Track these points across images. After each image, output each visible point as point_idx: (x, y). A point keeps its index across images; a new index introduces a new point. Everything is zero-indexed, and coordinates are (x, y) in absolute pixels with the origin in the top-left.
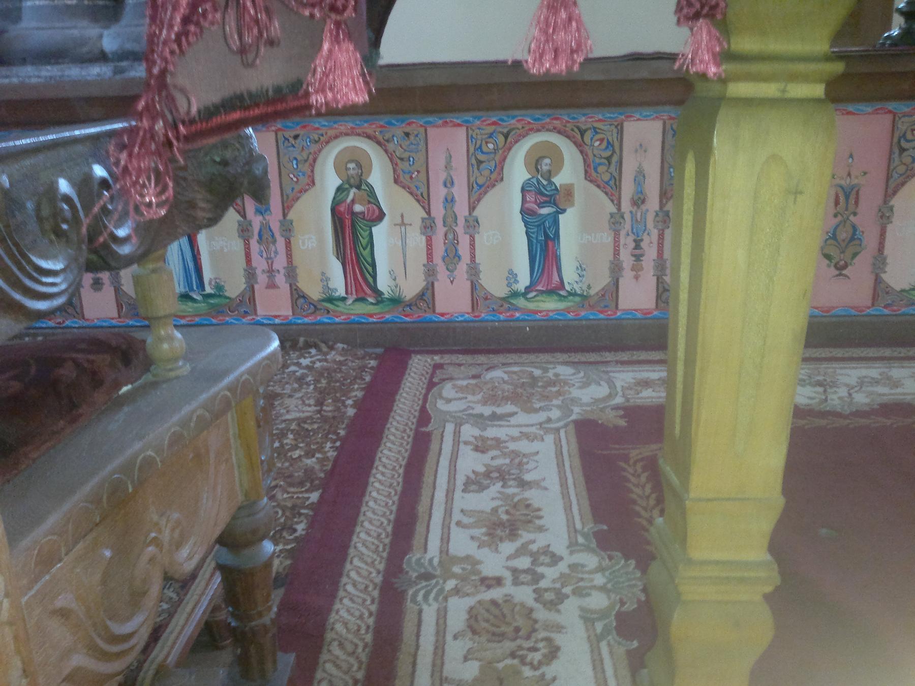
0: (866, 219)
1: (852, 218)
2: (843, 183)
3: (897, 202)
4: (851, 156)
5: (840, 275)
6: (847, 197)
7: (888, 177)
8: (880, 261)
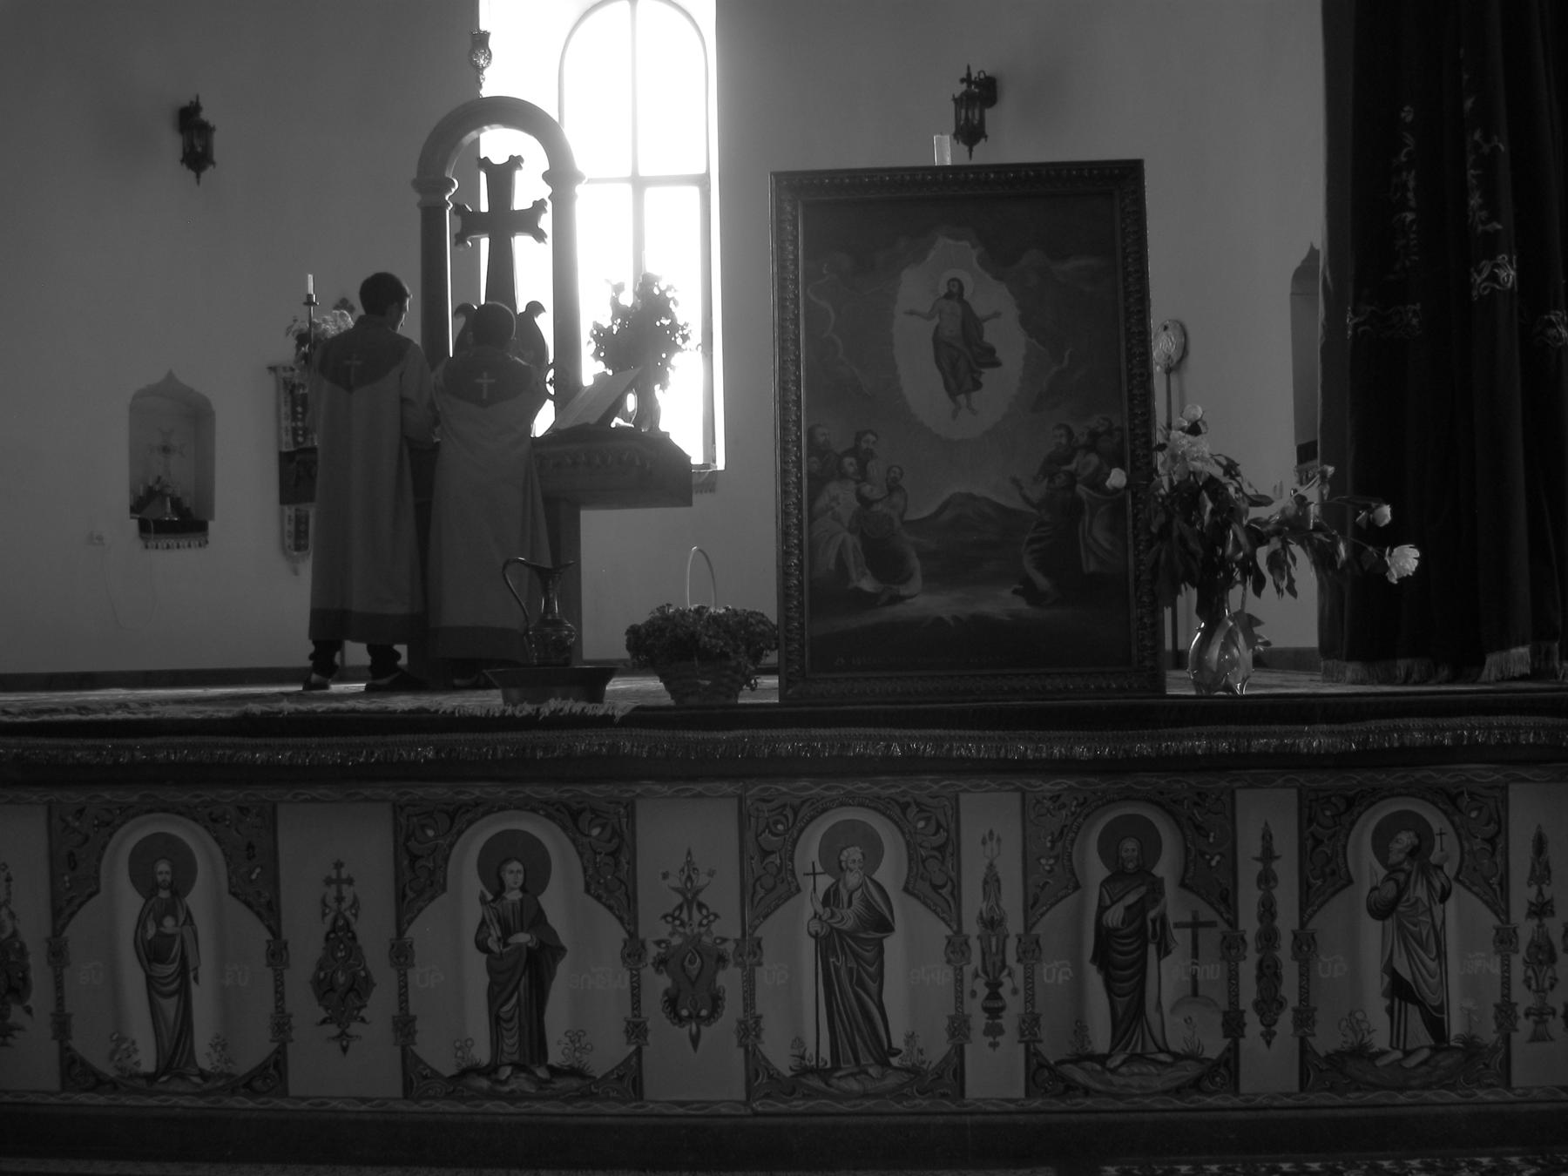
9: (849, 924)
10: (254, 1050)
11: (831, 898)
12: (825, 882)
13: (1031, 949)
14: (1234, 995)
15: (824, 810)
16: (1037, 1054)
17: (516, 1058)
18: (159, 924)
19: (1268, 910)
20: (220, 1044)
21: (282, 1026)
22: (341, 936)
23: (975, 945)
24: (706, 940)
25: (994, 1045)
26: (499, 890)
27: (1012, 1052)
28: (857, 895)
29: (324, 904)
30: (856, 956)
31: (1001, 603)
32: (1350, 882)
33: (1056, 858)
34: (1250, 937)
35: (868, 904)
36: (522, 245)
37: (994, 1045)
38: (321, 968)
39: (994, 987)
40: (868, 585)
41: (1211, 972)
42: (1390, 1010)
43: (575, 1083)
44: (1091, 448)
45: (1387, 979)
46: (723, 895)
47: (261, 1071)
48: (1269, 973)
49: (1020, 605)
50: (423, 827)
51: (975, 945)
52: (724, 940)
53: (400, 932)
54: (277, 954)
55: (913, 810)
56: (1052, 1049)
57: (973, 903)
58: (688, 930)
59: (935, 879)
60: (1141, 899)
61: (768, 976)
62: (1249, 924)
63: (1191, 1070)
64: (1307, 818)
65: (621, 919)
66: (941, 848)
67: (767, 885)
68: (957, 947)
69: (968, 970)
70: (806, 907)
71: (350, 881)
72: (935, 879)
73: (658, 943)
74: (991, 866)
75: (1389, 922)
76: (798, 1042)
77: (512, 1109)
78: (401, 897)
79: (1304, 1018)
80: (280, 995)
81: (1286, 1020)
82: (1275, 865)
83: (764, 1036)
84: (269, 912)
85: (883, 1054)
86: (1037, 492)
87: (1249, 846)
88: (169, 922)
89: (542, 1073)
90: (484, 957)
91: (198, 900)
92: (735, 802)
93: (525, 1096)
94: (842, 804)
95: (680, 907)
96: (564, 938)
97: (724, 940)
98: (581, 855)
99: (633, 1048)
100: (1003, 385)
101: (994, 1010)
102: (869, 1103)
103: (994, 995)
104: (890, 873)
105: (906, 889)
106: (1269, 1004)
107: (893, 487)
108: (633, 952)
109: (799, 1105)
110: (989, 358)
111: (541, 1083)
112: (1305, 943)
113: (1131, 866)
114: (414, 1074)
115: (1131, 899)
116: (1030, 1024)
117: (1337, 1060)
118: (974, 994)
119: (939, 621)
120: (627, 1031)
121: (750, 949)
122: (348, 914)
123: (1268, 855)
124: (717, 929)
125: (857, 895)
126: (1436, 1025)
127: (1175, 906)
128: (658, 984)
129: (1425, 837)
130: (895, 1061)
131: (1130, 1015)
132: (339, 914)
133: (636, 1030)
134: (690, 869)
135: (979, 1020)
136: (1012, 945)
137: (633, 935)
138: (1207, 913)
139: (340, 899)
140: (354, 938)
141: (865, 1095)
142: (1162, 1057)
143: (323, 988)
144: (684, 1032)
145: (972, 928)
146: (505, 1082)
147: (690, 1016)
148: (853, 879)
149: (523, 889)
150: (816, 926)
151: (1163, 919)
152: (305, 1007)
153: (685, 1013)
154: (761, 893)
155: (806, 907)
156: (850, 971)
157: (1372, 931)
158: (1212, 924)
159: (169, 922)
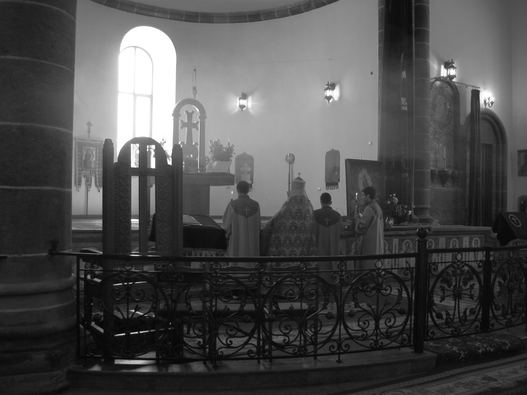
36: (194, 130)
64: (399, 242)
87: (394, 245)
123: (396, 247)
126: (409, 266)
129: (409, 244)
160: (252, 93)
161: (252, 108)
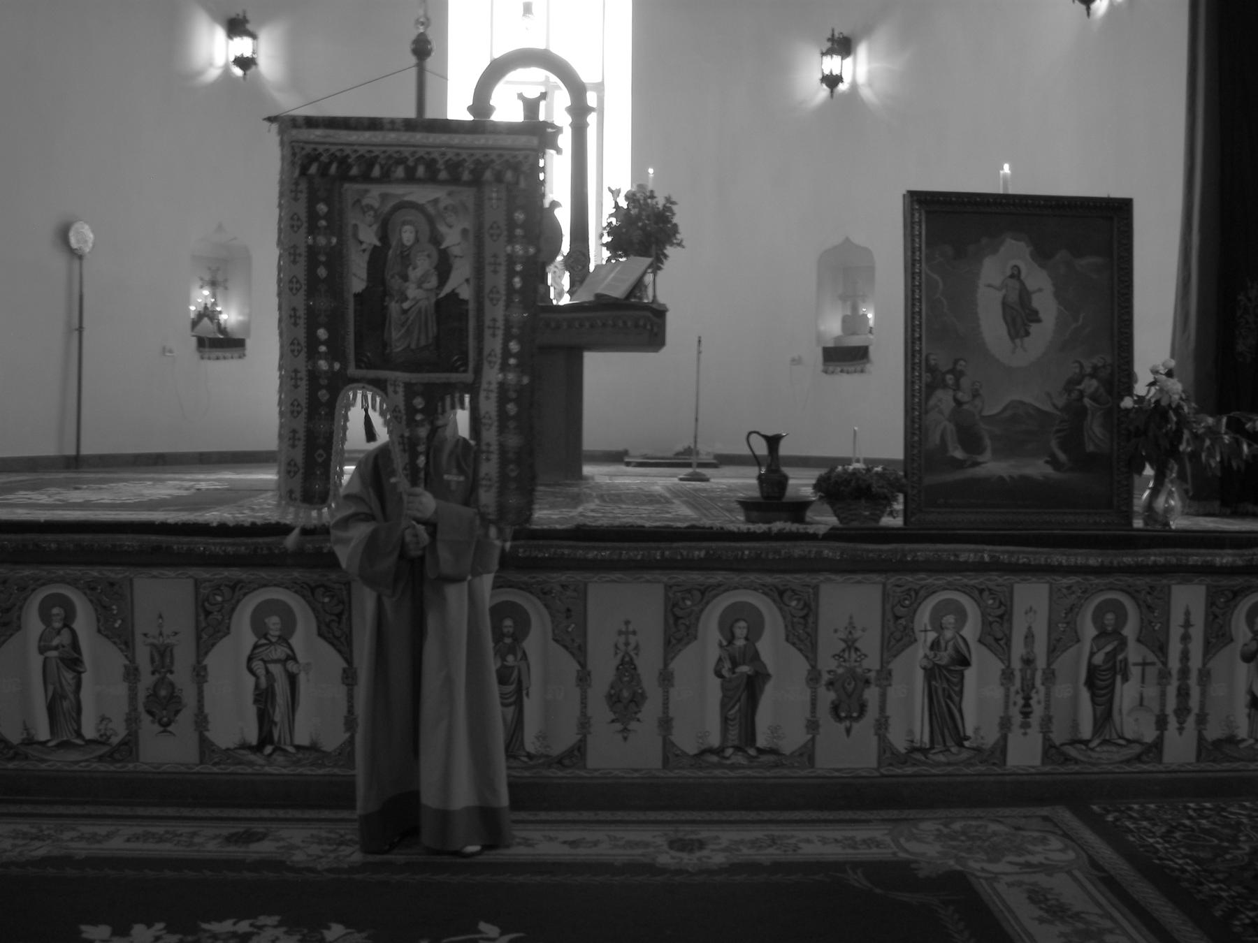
0: (181, 676)
1: (169, 676)
2: (155, 641)
3: (209, 661)
4: (160, 617)
5: (165, 731)
6: (162, 655)
7: (199, 638)
8: (201, 721)
9: (944, 662)
10: (565, 739)
11: (935, 645)
12: (932, 636)
13: (1050, 676)
14: (1163, 705)
15: (934, 592)
16: (1049, 739)
17: (736, 743)
18: (504, 659)
19: (1185, 656)
20: (542, 737)
21: (584, 724)
22: (627, 667)
23: (1018, 675)
24: (859, 670)
25: (1025, 734)
26: (731, 639)
27: (1035, 739)
28: (951, 644)
29: (616, 646)
30: (948, 680)
31: (1038, 469)
32: (1232, 640)
33: (1068, 623)
34: (1174, 672)
35: (957, 650)
37: (1025, 734)
38: (612, 687)
39: (1027, 699)
40: (959, 454)
41: (1152, 692)
42: (1249, 716)
43: (772, 758)
44: (1092, 376)
45: (1249, 697)
46: (870, 643)
47: (570, 753)
48: (1183, 693)
49: (1049, 470)
50: (684, 599)
51: (1018, 675)
52: (869, 671)
53: (666, 665)
54: (584, 678)
55: (986, 594)
56: (1058, 737)
57: (1018, 650)
58: (847, 665)
59: (997, 636)
60: (1115, 649)
61: (895, 692)
62: (1174, 664)
63: (1137, 749)
64: (1211, 603)
65: (807, 657)
66: (1001, 617)
67: (897, 636)
68: (1007, 675)
69: (1013, 689)
70: (919, 652)
71: (634, 633)
72: (997, 636)
73: (829, 672)
74: (1030, 628)
75: (1252, 664)
76: (911, 732)
77: (732, 774)
78: (668, 643)
79: (1202, 719)
80: (584, 703)
81: (1191, 721)
82: (1192, 631)
83: (891, 729)
84: (579, 652)
85: (960, 740)
86: (1061, 402)
87: (1177, 618)
88: (510, 658)
89: (752, 752)
90: (718, 681)
91: (532, 644)
92: (880, 587)
93: (742, 767)
94: (945, 589)
95: (844, 651)
96: (771, 670)
97: (869, 671)
98: (784, 618)
99: (809, 736)
100: (1043, 333)
101: (1026, 714)
102: (950, 769)
103: (1027, 705)
104: (971, 631)
105: (980, 641)
106: (1183, 711)
107: (976, 395)
108: (814, 677)
109: (909, 770)
110: (1034, 317)
111: (751, 758)
112: (1205, 676)
113: (1110, 629)
114: (670, 753)
115: (1109, 648)
116: (1047, 721)
117: (1218, 743)
118: (1015, 704)
119: (1001, 478)
120: (807, 727)
121: (885, 675)
122: (632, 653)
123: (1187, 624)
124: (866, 664)
125: (951, 644)
127: (1134, 653)
128: (827, 697)
130: (967, 744)
131: (1104, 718)
132: (627, 653)
133: (813, 726)
134: (851, 626)
135: (1017, 719)
136: (1039, 675)
137: (814, 667)
138: (1151, 658)
139: (627, 644)
140: (635, 669)
141: (949, 764)
142: (1122, 742)
143: (613, 699)
144: (842, 727)
145: (1017, 664)
146: (728, 758)
147: (846, 718)
148: (949, 634)
149: (747, 639)
150: (925, 663)
151: (1126, 660)
152: (600, 712)
153: (843, 715)
154: (893, 642)
155: (919, 652)
156: (944, 689)
157: (1243, 669)
158: (1153, 664)
159: (510, 658)
160: (867, 31)
161: (870, 84)
